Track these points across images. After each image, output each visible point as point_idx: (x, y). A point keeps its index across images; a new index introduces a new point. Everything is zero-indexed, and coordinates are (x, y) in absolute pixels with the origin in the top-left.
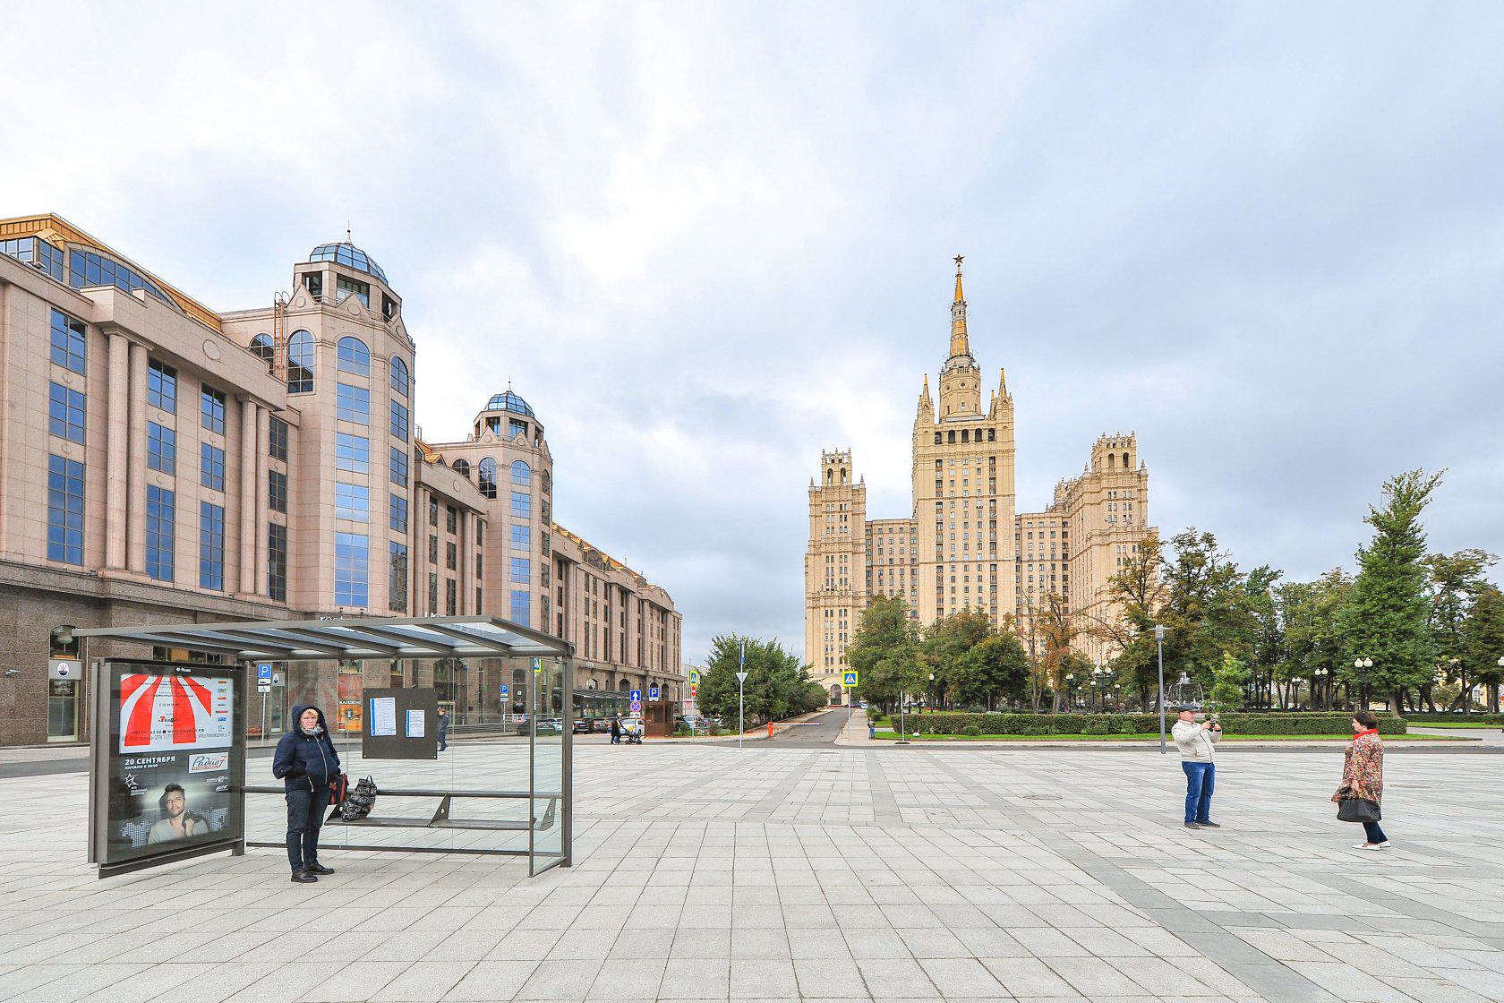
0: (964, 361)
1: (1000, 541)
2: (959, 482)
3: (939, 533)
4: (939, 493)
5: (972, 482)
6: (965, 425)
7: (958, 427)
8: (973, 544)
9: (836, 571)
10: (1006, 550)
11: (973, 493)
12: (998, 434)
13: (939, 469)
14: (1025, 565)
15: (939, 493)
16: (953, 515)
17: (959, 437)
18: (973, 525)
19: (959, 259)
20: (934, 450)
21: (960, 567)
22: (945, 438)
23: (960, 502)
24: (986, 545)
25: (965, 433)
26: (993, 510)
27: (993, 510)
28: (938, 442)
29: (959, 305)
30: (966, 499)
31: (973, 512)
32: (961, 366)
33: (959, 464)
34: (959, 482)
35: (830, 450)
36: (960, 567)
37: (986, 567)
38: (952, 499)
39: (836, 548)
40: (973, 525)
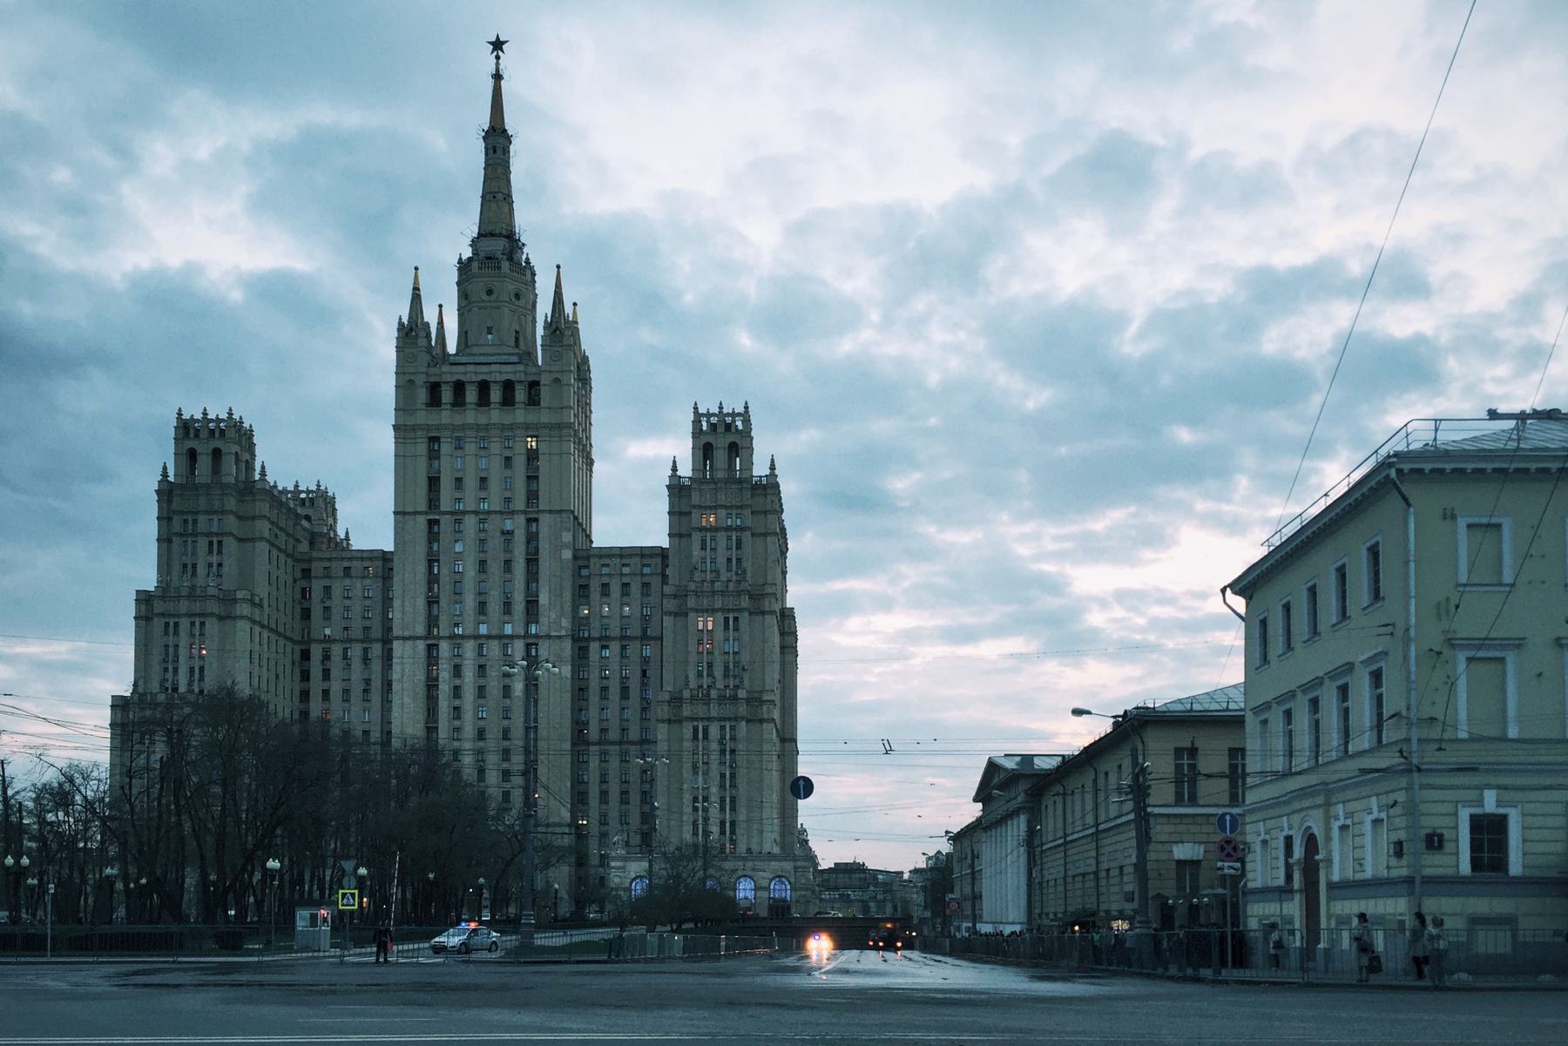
0: (499, 245)
1: (544, 599)
2: (471, 483)
3: (432, 579)
4: (433, 503)
5: (495, 485)
6: (483, 373)
7: (471, 375)
8: (494, 607)
9: (183, 652)
10: (555, 616)
11: (495, 503)
12: (545, 394)
13: (434, 455)
14: (594, 647)
15: (433, 503)
16: (462, 550)
17: (471, 395)
18: (495, 568)
19: (498, 45)
20: (422, 417)
21: (469, 648)
22: (447, 395)
23: (470, 522)
24: (519, 607)
25: (484, 387)
26: (532, 538)
27: (532, 538)
28: (434, 401)
29: (497, 140)
30: (483, 516)
31: (495, 542)
32: (496, 260)
33: (470, 448)
34: (471, 483)
35: (193, 411)
36: (469, 648)
37: (518, 648)
38: (458, 516)
39: (184, 606)
40: (495, 568)
